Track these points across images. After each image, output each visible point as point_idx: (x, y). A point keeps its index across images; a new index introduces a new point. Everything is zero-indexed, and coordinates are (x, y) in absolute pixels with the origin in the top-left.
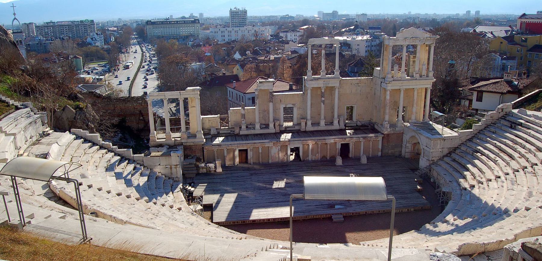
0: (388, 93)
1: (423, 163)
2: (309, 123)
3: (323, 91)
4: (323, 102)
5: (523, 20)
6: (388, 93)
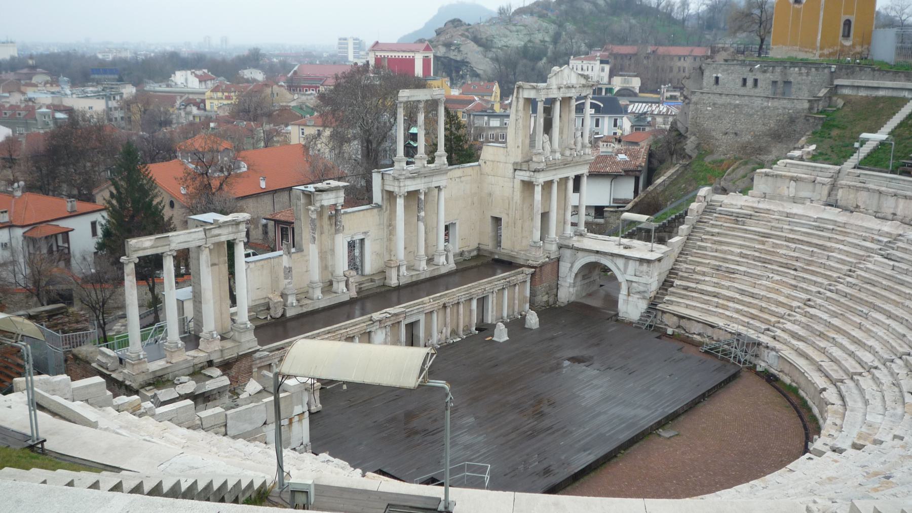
0: (538, 190)
1: (631, 308)
2: (403, 270)
3: (422, 197)
4: (424, 220)
5: (379, 54)
6: (538, 190)
